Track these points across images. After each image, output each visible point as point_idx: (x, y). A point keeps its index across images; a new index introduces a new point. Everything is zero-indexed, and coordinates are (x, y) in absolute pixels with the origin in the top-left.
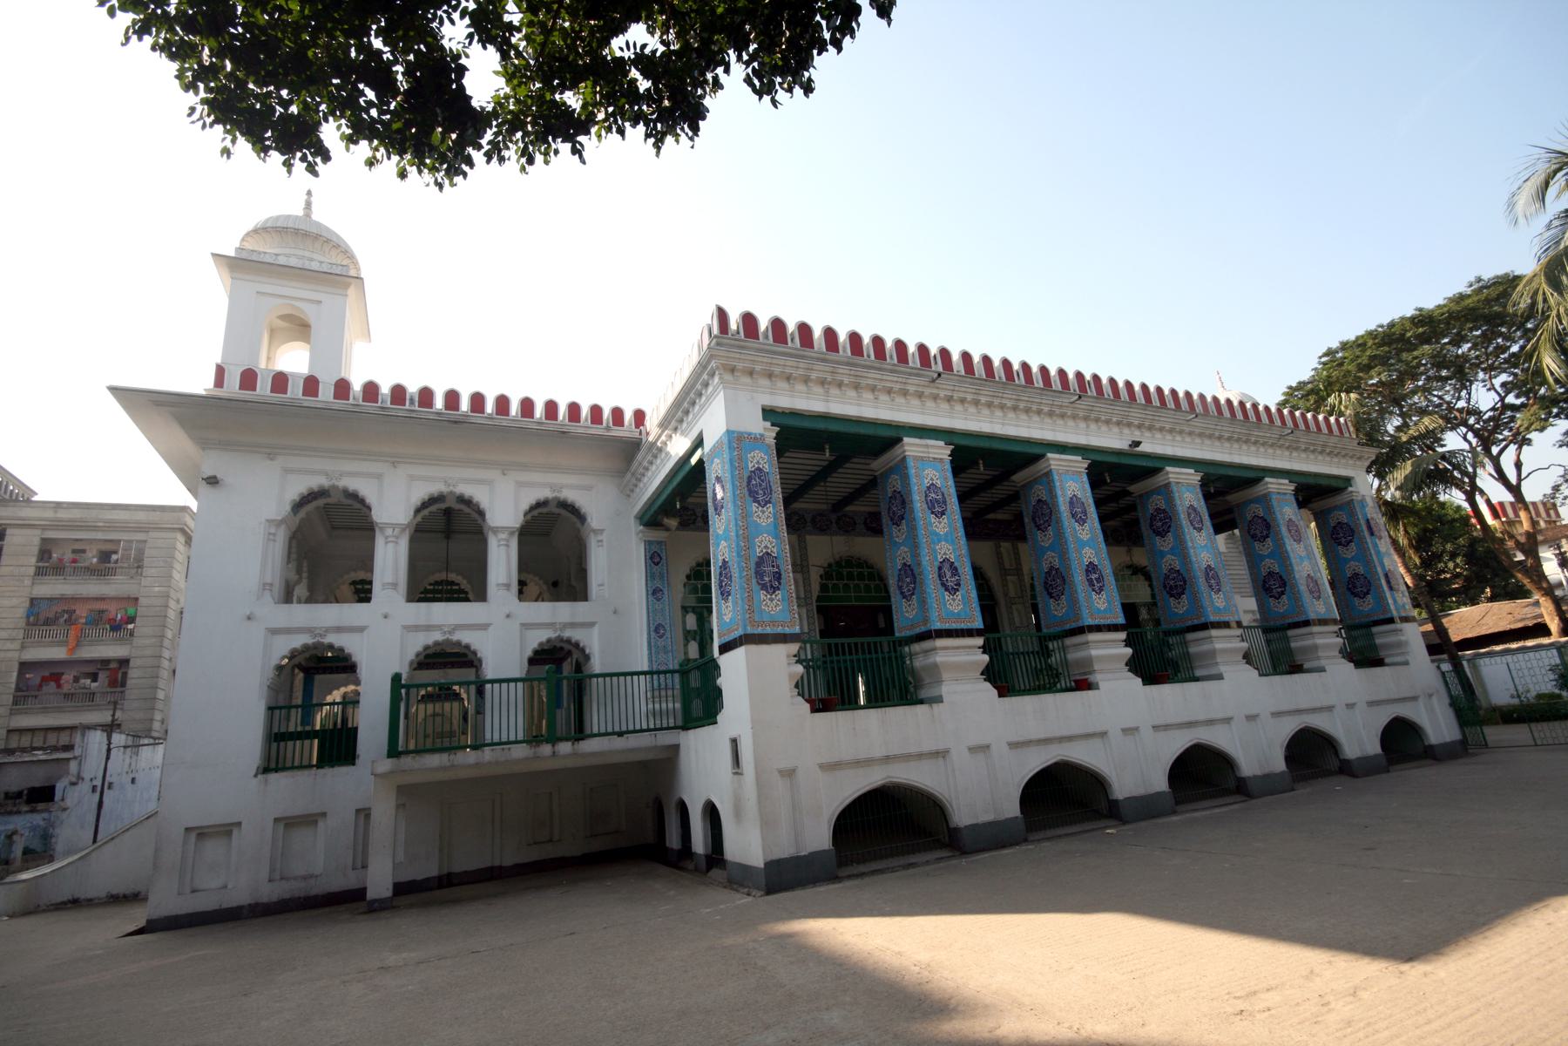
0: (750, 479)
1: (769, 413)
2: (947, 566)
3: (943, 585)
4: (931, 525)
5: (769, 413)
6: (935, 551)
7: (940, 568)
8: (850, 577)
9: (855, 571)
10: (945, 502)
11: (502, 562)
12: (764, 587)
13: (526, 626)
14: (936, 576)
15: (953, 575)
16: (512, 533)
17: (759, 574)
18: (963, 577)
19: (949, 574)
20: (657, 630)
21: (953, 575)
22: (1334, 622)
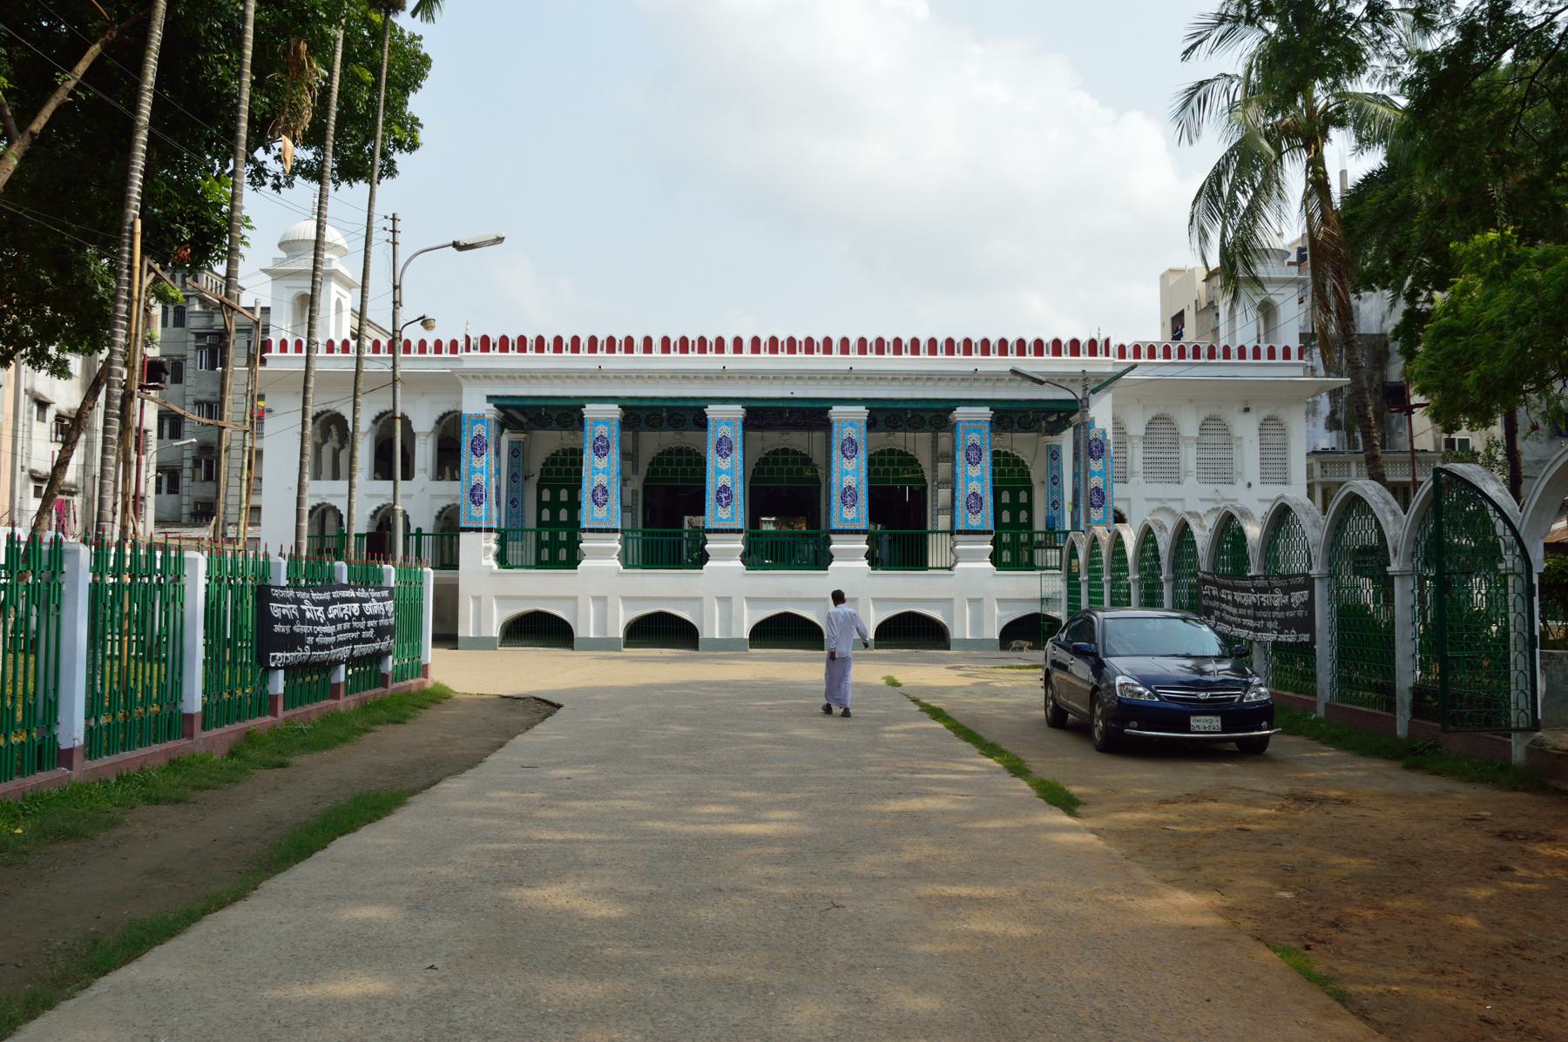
0: (473, 441)
1: (490, 398)
2: (600, 489)
3: (594, 501)
4: (593, 462)
5: (490, 398)
6: (593, 479)
7: (594, 491)
8: (679, 462)
9: (684, 458)
10: (608, 447)
11: (425, 453)
12: (474, 502)
13: (434, 497)
14: (590, 495)
15: (603, 495)
16: (427, 436)
17: (472, 495)
18: (610, 496)
19: (600, 494)
20: (512, 502)
21: (603, 495)
22: (989, 532)
